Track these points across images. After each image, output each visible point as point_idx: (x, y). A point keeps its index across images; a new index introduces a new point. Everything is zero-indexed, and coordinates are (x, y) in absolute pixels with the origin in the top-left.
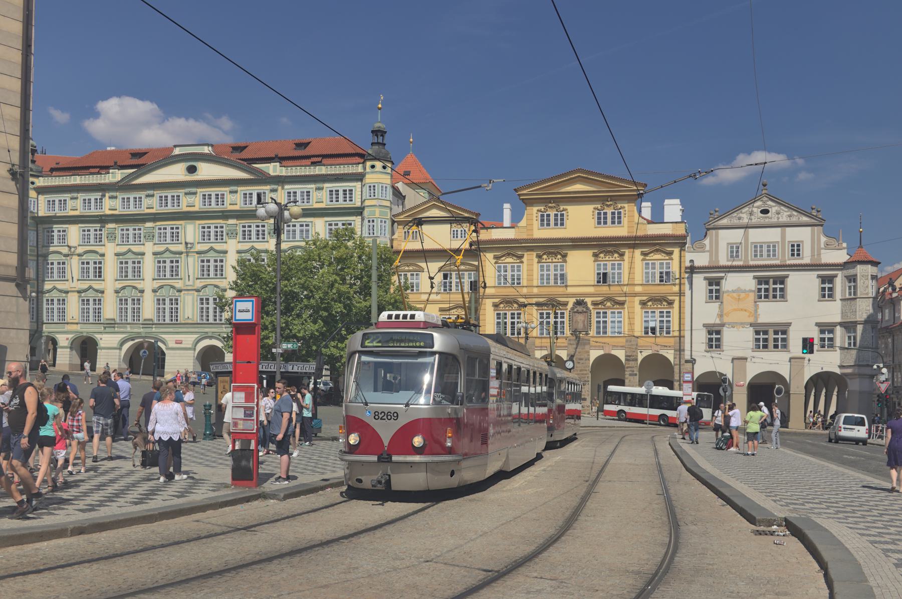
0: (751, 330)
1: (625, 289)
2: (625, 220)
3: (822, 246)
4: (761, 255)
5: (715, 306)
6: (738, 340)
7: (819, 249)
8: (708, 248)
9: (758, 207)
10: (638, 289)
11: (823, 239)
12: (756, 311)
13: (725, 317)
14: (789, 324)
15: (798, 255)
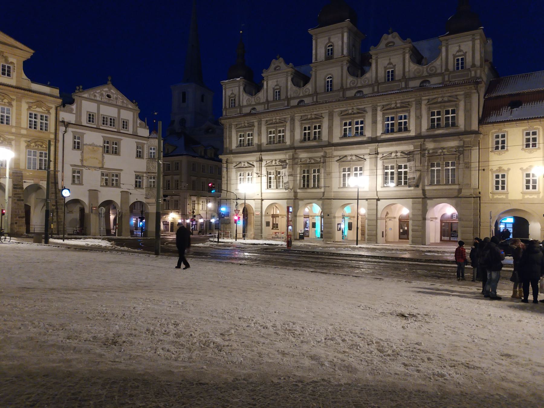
0: (98, 173)
1: (13, 130)
2: (14, 74)
3: (138, 125)
4: (107, 124)
5: (78, 152)
6: (92, 179)
7: (137, 127)
8: (74, 112)
9: (106, 91)
10: (24, 132)
11: (139, 121)
12: (103, 160)
13: (84, 161)
14: (121, 170)
15: (126, 128)
